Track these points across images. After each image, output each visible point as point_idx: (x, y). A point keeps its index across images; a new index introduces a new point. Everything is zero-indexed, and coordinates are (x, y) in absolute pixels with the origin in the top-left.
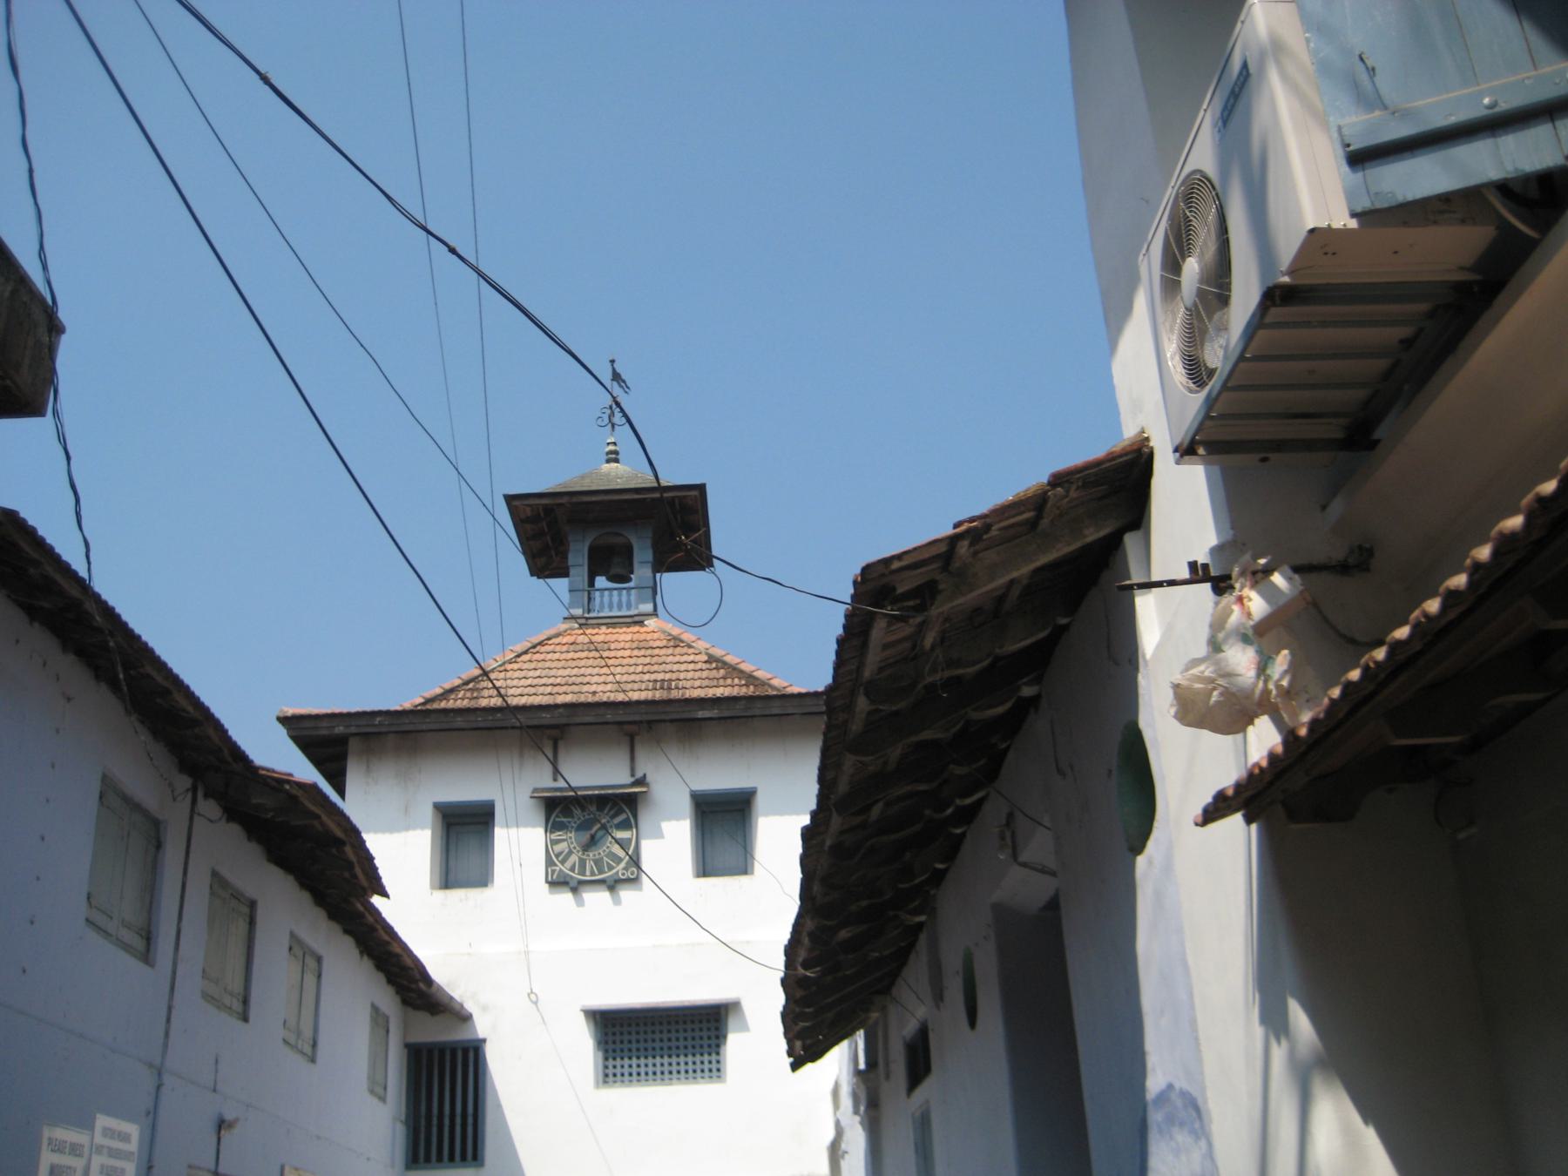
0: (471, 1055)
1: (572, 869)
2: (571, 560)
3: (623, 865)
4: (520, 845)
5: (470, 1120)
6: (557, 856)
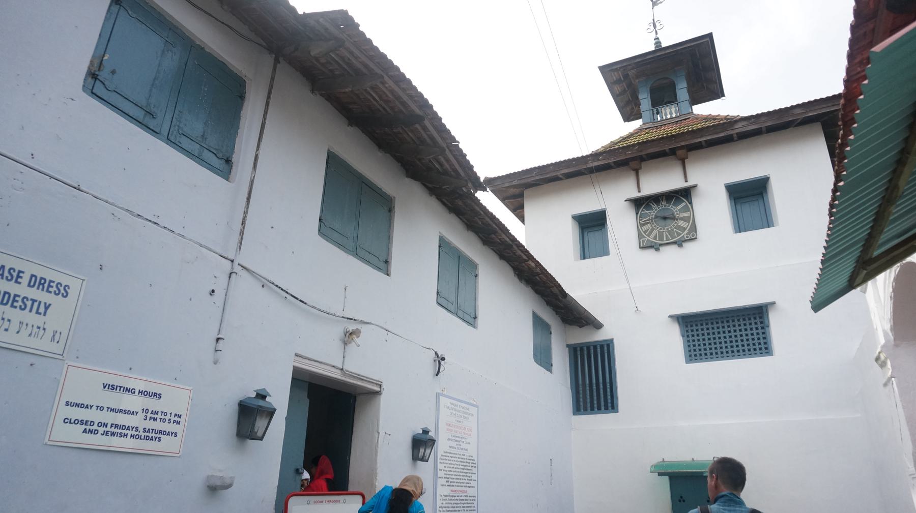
0: (606, 349)
1: (655, 238)
2: (641, 97)
3: (686, 232)
5: (608, 386)
6: (645, 232)
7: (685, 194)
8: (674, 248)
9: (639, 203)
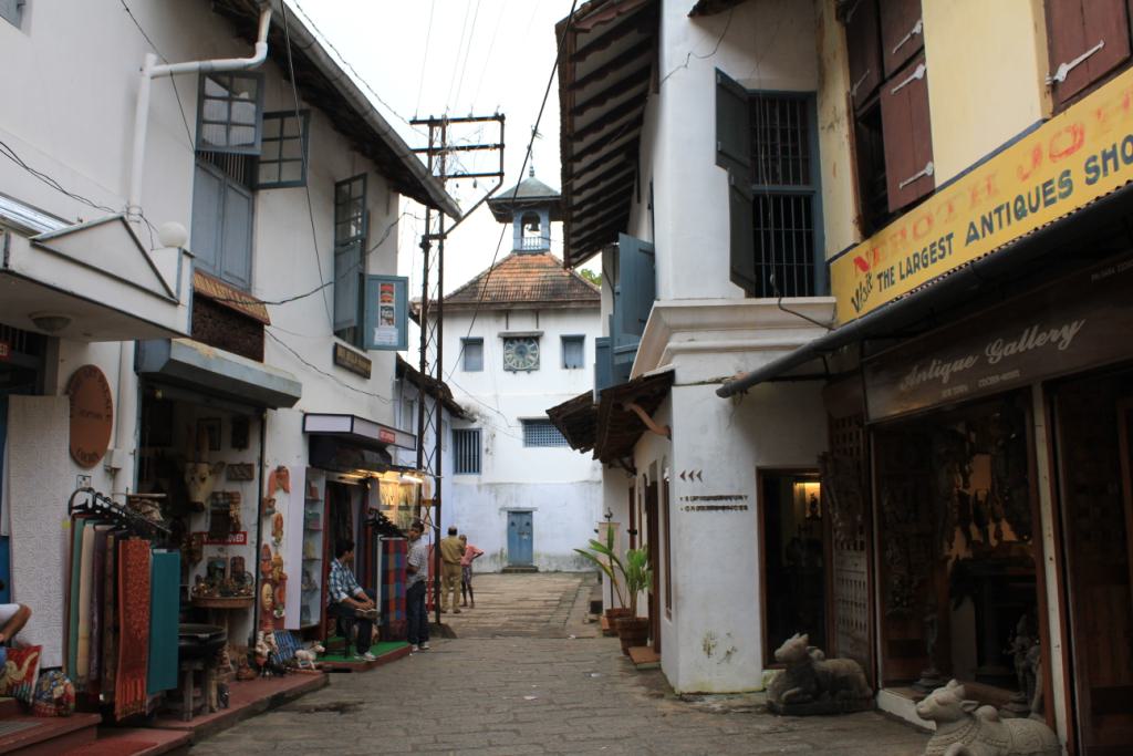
4: (494, 351)
7: (534, 339)
8: (525, 373)
9: (508, 339)
